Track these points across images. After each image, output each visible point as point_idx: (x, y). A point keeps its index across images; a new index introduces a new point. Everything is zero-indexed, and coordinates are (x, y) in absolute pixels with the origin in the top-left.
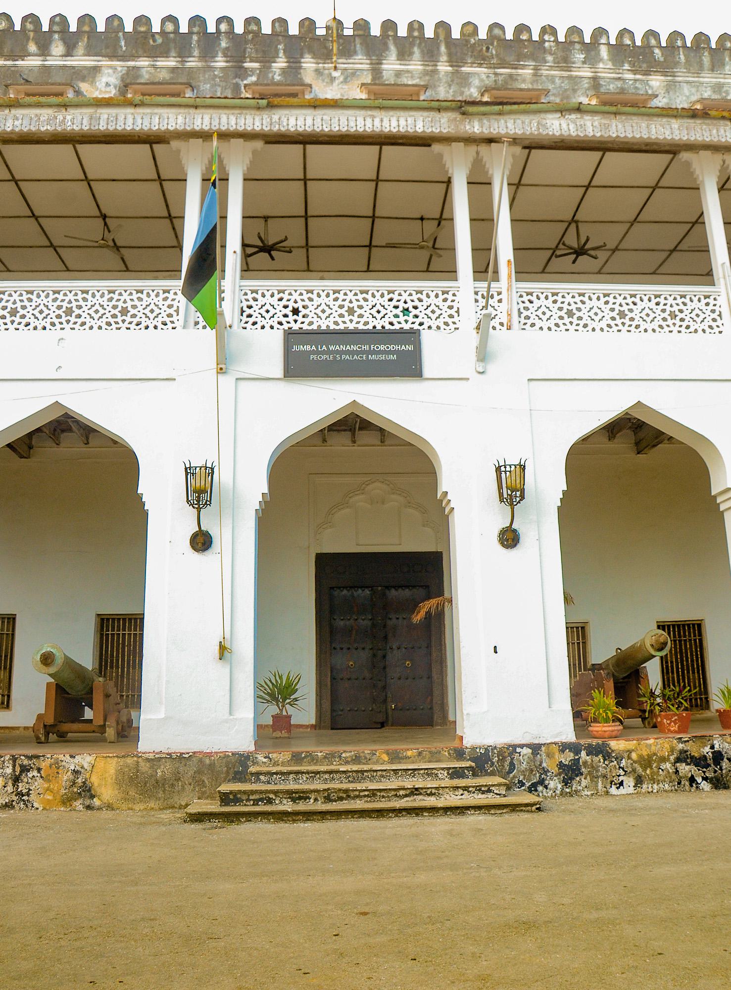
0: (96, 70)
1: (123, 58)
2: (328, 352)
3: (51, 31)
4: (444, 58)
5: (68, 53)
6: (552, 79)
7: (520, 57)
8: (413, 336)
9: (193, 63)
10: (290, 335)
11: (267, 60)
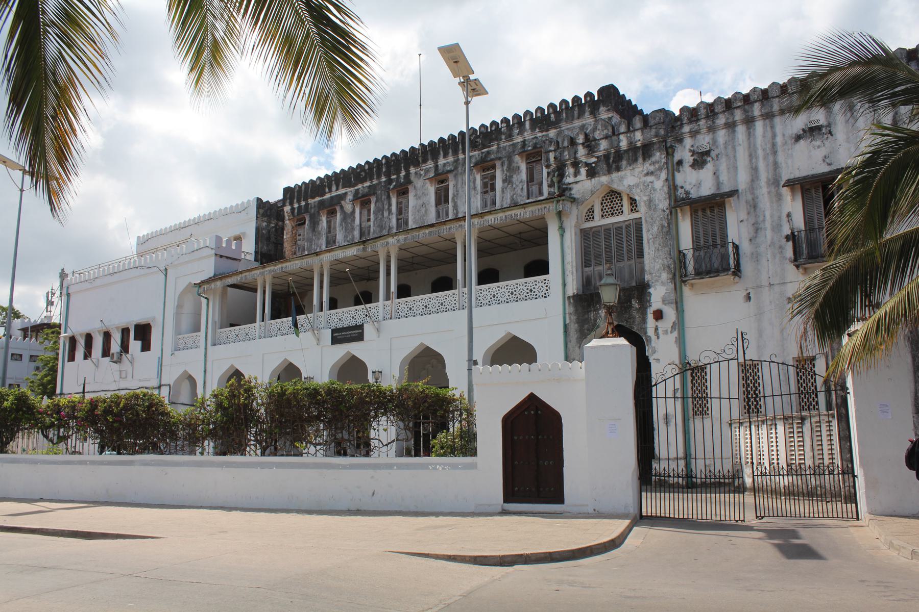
0: (346, 194)
1: (354, 186)
5: (337, 189)
6: (504, 148)
7: (492, 140)
9: (375, 182)
10: (333, 331)
11: (398, 173)
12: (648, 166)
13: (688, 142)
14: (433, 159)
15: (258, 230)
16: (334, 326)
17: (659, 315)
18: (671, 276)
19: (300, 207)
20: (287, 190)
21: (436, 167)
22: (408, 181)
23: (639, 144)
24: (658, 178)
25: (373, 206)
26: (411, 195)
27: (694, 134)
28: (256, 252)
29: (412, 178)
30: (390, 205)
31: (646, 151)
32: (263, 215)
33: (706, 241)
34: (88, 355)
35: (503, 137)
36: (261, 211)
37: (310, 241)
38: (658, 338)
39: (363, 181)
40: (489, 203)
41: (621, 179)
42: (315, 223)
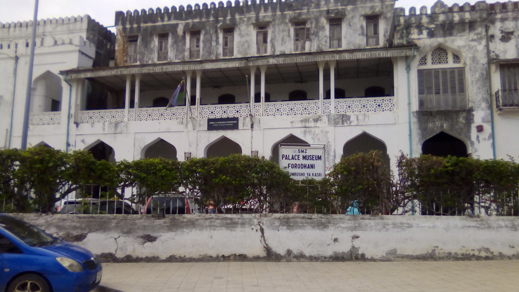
2: (217, 124)
3: (164, 13)
4: (278, 10)
5: (169, 19)
6: (313, 12)
8: (237, 119)
9: (204, 20)
10: (209, 120)
11: (225, 16)
12: (472, 36)
13: (498, 25)
14: (255, 11)
17: (480, 129)
18: (488, 105)
23: (467, 21)
24: (480, 44)
25: (202, 37)
26: (236, 34)
27: (503, 20)
30: (217, 38)
31: (471, 25)
33: (510, 86)
35: (313, 5)
37: (143, 55)
38: (479, 142)
40: (299, 47)
41: (453, 41)
42: (146, 43)
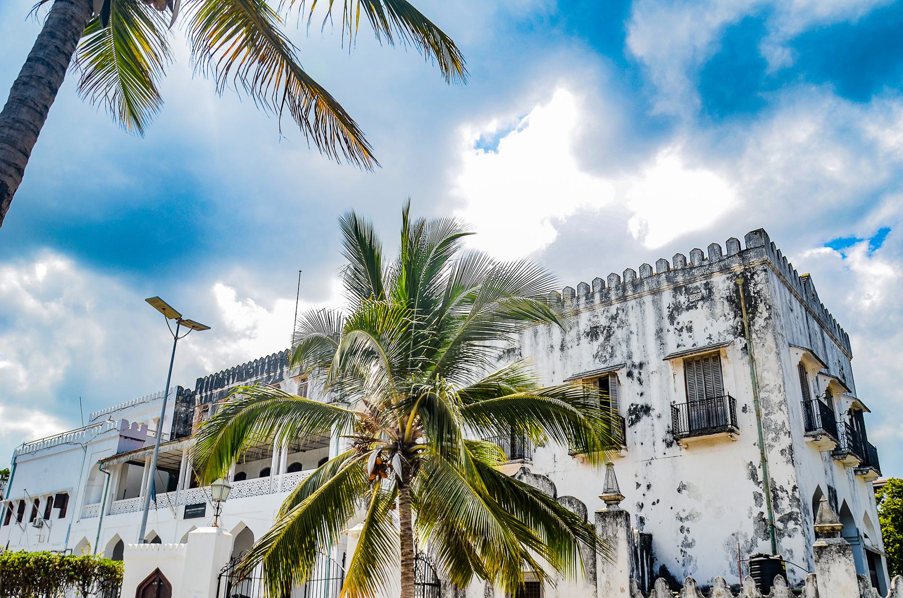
10: (187, 507)
11: (275, 372)
15: (176, 413)
16: (190, 503)
19: (206, 396)
20: (200, 381)
21: (301, 367)
22: (281, 379)
28: (172, 434)
29: (284, 376)
32: (182, 401)
34: (20, 519)
36: (181, 398)
39: (251, 376)
